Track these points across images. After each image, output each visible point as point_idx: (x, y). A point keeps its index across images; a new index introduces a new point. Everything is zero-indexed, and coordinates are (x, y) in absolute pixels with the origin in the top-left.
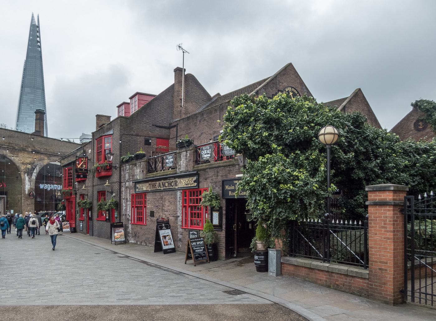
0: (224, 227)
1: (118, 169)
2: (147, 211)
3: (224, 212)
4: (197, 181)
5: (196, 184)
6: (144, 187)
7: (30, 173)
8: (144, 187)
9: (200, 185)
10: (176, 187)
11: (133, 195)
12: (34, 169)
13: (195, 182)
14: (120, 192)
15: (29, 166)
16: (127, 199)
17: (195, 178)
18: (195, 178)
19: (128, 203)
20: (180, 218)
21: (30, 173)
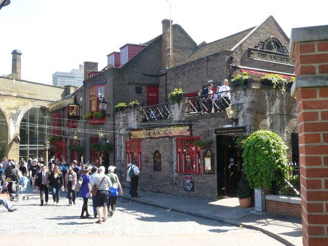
0: (216, 170)
1: (112, 117)
2: (142, 157)
3: (215, 158)
4: (191, 130)
5: (189, 133)
6: (141, 134)
7: (14, 117)
8: (141, 134)
9: (193, 133)
10: (171, 135)
11: (126, 143)
12: (18, 114)
13: (188, 130)
14: (114, 139)
15: (14, 111)
16: (121, 146)
17: (188, 128)
18: (188, 128)
19: (123, 149)
20: (175, 163)
21: (14, 117)
